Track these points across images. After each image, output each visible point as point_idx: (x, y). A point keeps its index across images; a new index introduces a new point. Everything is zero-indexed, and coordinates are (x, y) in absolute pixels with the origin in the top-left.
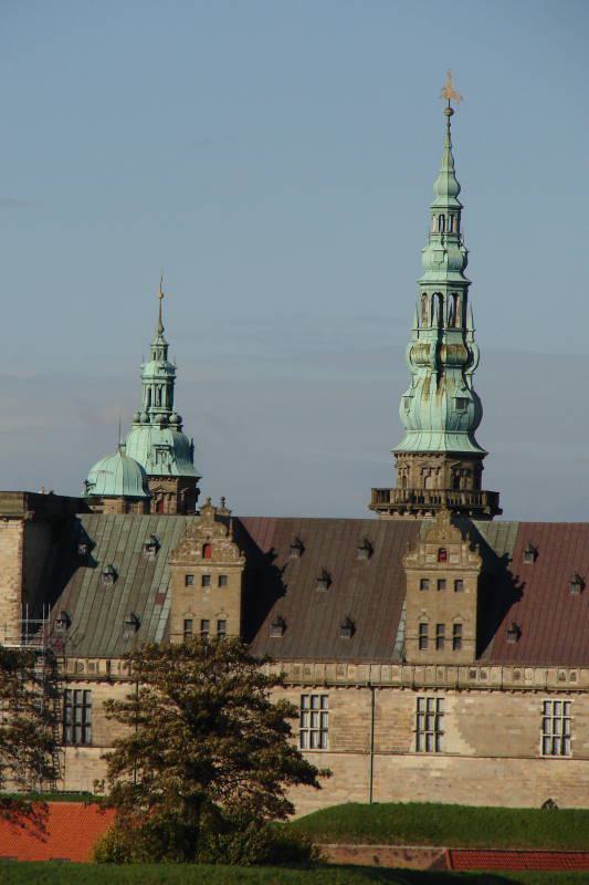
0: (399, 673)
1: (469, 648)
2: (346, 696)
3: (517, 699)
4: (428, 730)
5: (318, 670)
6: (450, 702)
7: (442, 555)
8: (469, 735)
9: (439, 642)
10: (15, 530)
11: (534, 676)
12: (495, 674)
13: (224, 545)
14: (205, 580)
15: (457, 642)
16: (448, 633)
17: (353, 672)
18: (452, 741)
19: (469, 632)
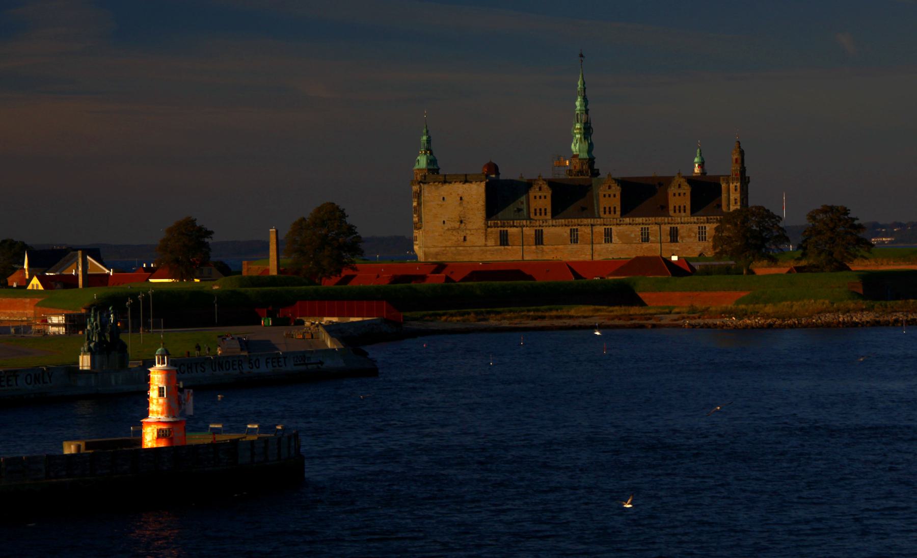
0: (599, 221)
1: (618, 213)
2: (583, 228)
3: (634, 227)
4: (608, 236)
5: (575, 221)
6: (614, 228)
7: (610, 187)
8: (620, 238)
9: (610, 213)
10: (483, 184)
11: (639, 220)
12: (627, 220)
13: (545, 186)
14: (540, 197)
15: (615, 213)
16: (612, 209)
17: (586, 221)
18: (615, 238)
19: (618, 209)
